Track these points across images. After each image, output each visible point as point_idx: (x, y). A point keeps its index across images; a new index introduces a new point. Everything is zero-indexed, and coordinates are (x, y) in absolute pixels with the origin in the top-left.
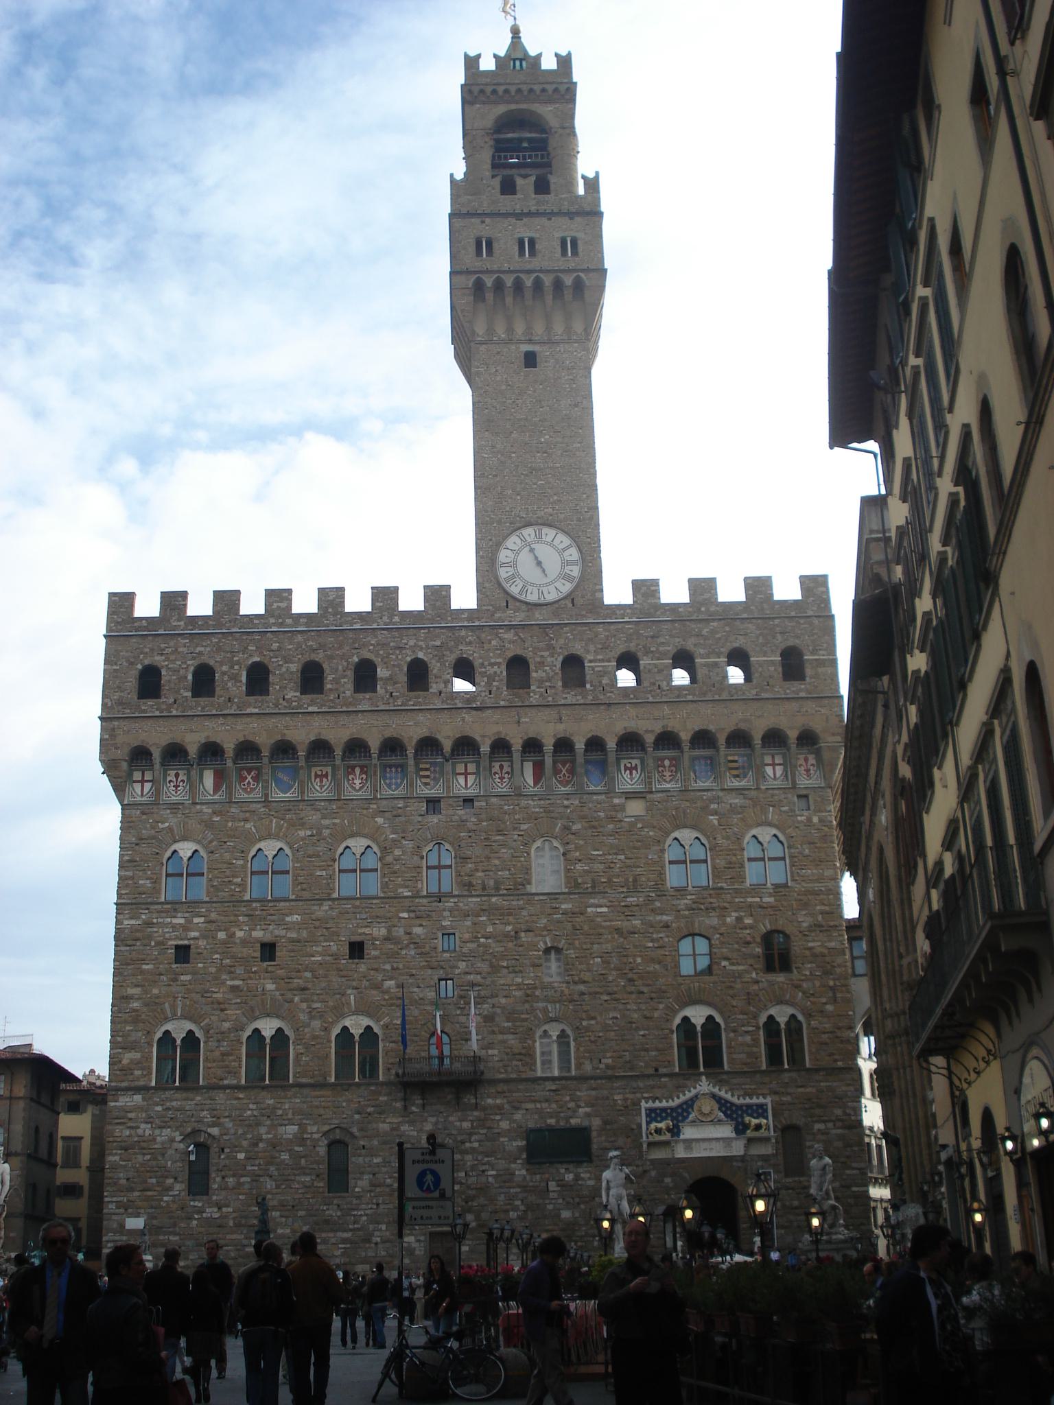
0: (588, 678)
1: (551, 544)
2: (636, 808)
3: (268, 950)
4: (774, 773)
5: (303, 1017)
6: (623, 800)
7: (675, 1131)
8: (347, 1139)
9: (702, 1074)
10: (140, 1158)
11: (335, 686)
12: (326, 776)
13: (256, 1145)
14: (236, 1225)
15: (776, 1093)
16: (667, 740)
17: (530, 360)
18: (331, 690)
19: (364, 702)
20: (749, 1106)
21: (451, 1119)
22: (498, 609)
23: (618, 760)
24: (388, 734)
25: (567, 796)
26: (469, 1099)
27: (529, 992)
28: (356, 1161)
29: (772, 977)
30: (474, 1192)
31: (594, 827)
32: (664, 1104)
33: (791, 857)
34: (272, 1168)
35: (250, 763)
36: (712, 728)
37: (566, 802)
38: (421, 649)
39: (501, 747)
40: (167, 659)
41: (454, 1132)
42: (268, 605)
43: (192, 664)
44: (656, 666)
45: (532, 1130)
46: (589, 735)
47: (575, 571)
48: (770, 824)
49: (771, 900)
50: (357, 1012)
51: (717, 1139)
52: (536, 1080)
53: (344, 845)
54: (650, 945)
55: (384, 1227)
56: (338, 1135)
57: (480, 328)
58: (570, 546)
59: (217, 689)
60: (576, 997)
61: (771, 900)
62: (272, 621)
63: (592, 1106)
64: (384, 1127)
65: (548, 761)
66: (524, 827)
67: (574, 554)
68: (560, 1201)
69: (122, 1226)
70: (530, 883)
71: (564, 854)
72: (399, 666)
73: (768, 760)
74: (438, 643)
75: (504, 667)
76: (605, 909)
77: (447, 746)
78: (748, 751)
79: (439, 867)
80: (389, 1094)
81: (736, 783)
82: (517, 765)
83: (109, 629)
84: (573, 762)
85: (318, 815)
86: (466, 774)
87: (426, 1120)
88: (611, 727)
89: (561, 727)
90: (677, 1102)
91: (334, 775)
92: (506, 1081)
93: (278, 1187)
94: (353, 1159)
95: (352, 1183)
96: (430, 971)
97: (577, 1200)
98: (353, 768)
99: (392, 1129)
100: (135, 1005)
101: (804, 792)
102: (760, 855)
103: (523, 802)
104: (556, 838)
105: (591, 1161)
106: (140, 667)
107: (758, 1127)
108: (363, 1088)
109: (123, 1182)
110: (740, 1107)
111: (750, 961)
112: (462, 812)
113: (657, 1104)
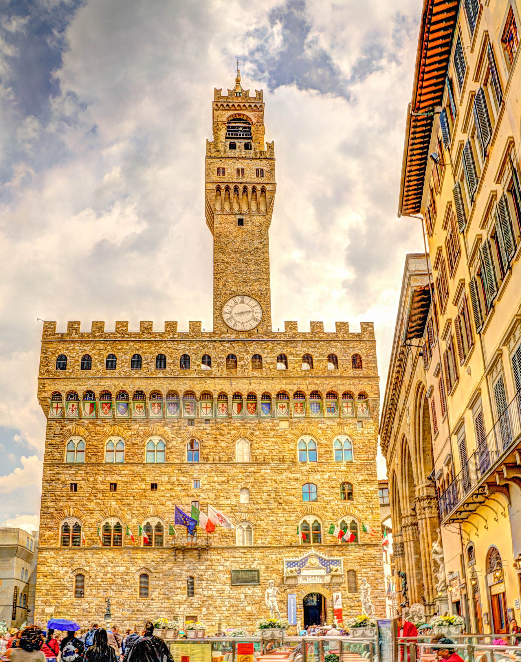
0: (264, 365)
1: (248, 304)
2: (284, 425)
3: (114, 486)
5: (129, 517)
6: (278, 421)
7: (299, 571)
8: (148, 573)
9: (311, 546)
10: (52, 580)
12: (142, 407)
13: (106, 575)
14: (96, 611)
16: (299, 394)
17: (241, 222)
19: (160, 374)
20: (333, 561)
22: (224, 333)
23: (277, 403)
27: (233, 508)
28: (152, 583)
29: (344, 503)
31: (264, 433)
32: (294, 559)
33: (354, 449)
34: (113, 586)
35: (107, 401)
36: (320, 389)
40: (70, 352)
42: (117, 328)
47: (259, 317)
50: (153, 516)
51: (318, 576)
52: (235, 548)
55: (164, 613)
56: (144, 571)
57: (218, 207)
60: (255, 510)
62: (119, 335)
63: (262, 560)
64: (165, 568)
66: (232, 432)
67: (258, 309)
69: (43, 611)
71: (251, 445)
72: (176, 357)
73: (345, 405)
74: (195, 347)
75: (225, 359)
76: (269, 471)
77: (198, 395)
78: (336, 400)
82: (230, 403)
83: (44, 338)
84: (256, 403)
86: (206, 408)
88: (273, 387)
89: (251, 387)
90: (300, 558)
91: (145, 407)
92: (223, 548)
93: (115, 594)
95: (150, 593)
96: (188, 498)
98: (154, 404)
100: (51, 510)
102: (340, 448)
103: (232, 422)
104: (247, 438)
106: (57, 355)
107: (336, 571)
109: (45, 591)
110: (329, 561)
111: (335, 496)
113: (291, 559)
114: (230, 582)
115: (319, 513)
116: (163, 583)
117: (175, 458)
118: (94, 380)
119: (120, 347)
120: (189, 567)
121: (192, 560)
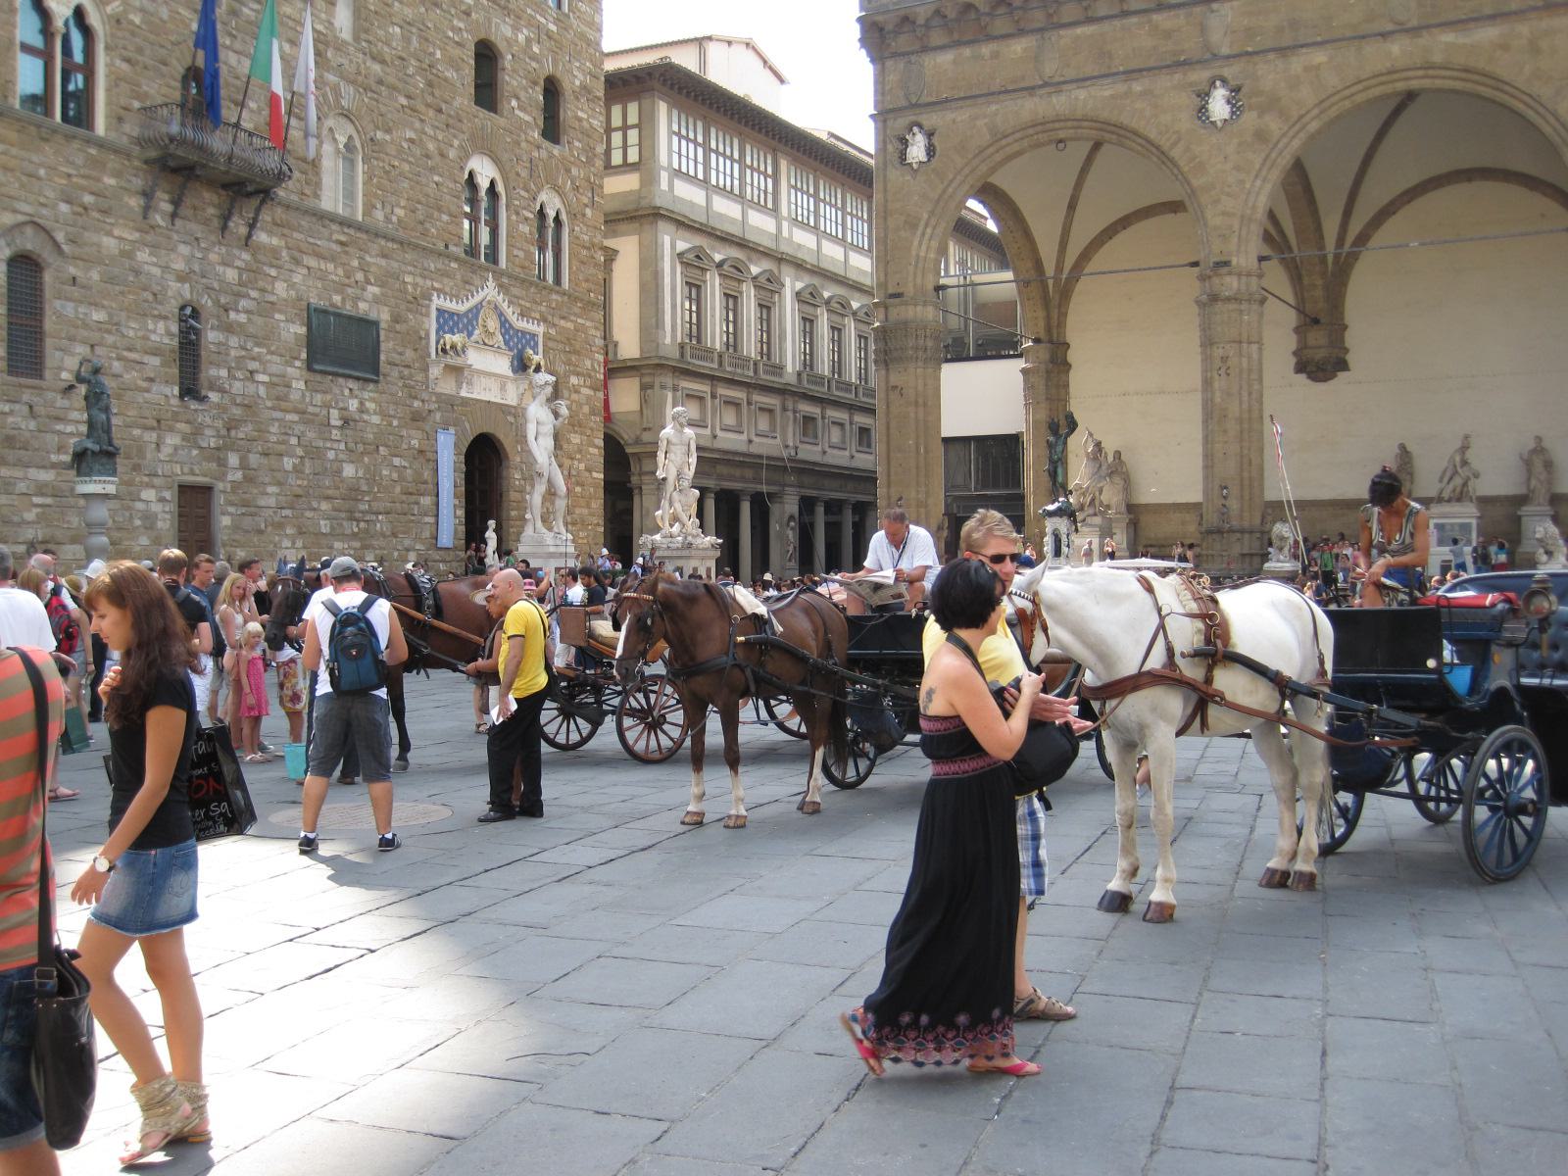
8: (47, 255)
15: (545, 321)
20: (524, 333)
21: (213, 257)
26: (238, 226)
28: (59, 310)
29: (546, 144)
30: (237, 412)
41: (216, 285)
45: (315, 310)
49: (553, 28)
54: (451, 34)
56: (29, 242)
61: (553, 28)
68: (342, 446)
80: (117, 174)
87: (173, 250)
92: (288, 207)
94: (58, 304)
97: (361, 448)
99: (124, 254)
105: (377, 382)
108: (76, 144)
114: (304, 356)
115: (505, 157)
116: (98, 316)
120: (189, 260)
121: (198, 230)
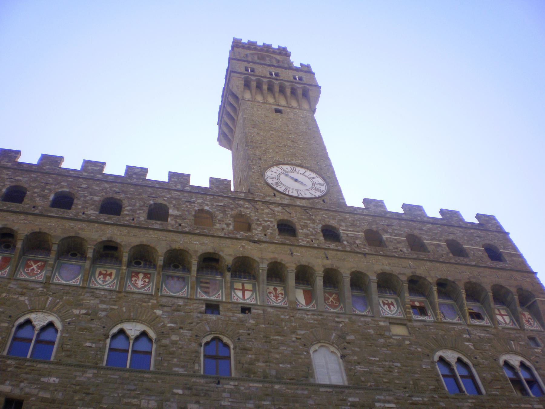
0: (344, 238)
2: (399, 331)
4: (504, 319)
6: (388, 325)
11: (131, 213)
12: (110, 275)
18: (127, 215)
19: (157, 224)
22: (269, 196)
24: (176, 246)
25: (338, 315)
36: (450, 278)
37: (337, 319)
38: (207, 205)
39: (276, 273)
43: (8, 184)
44: (395, 240)
46: (353, 270)
47: (324, 188)
48: (516, 353)
53: (119, 327)
58: (317, 177)
59: (26, 200)
65: (319, 282)
70: (313, 376)
71: (343, 357)
74: (222, 204)
75: (275, 224)
79: (216, 358)
81: (477, 322)
85: (98, 302)
86: (243, 290)
98: (137, 274)
101: (532, 334)
103: (298, 315)
104: (332, 344)
112: (241, 315)
117: (178, 366)
118: (22, 217)
119: (84, 186)
